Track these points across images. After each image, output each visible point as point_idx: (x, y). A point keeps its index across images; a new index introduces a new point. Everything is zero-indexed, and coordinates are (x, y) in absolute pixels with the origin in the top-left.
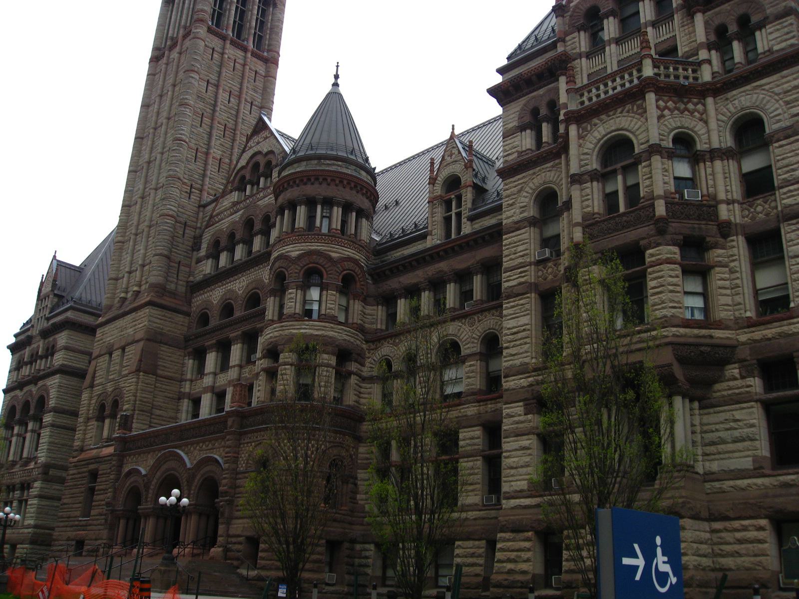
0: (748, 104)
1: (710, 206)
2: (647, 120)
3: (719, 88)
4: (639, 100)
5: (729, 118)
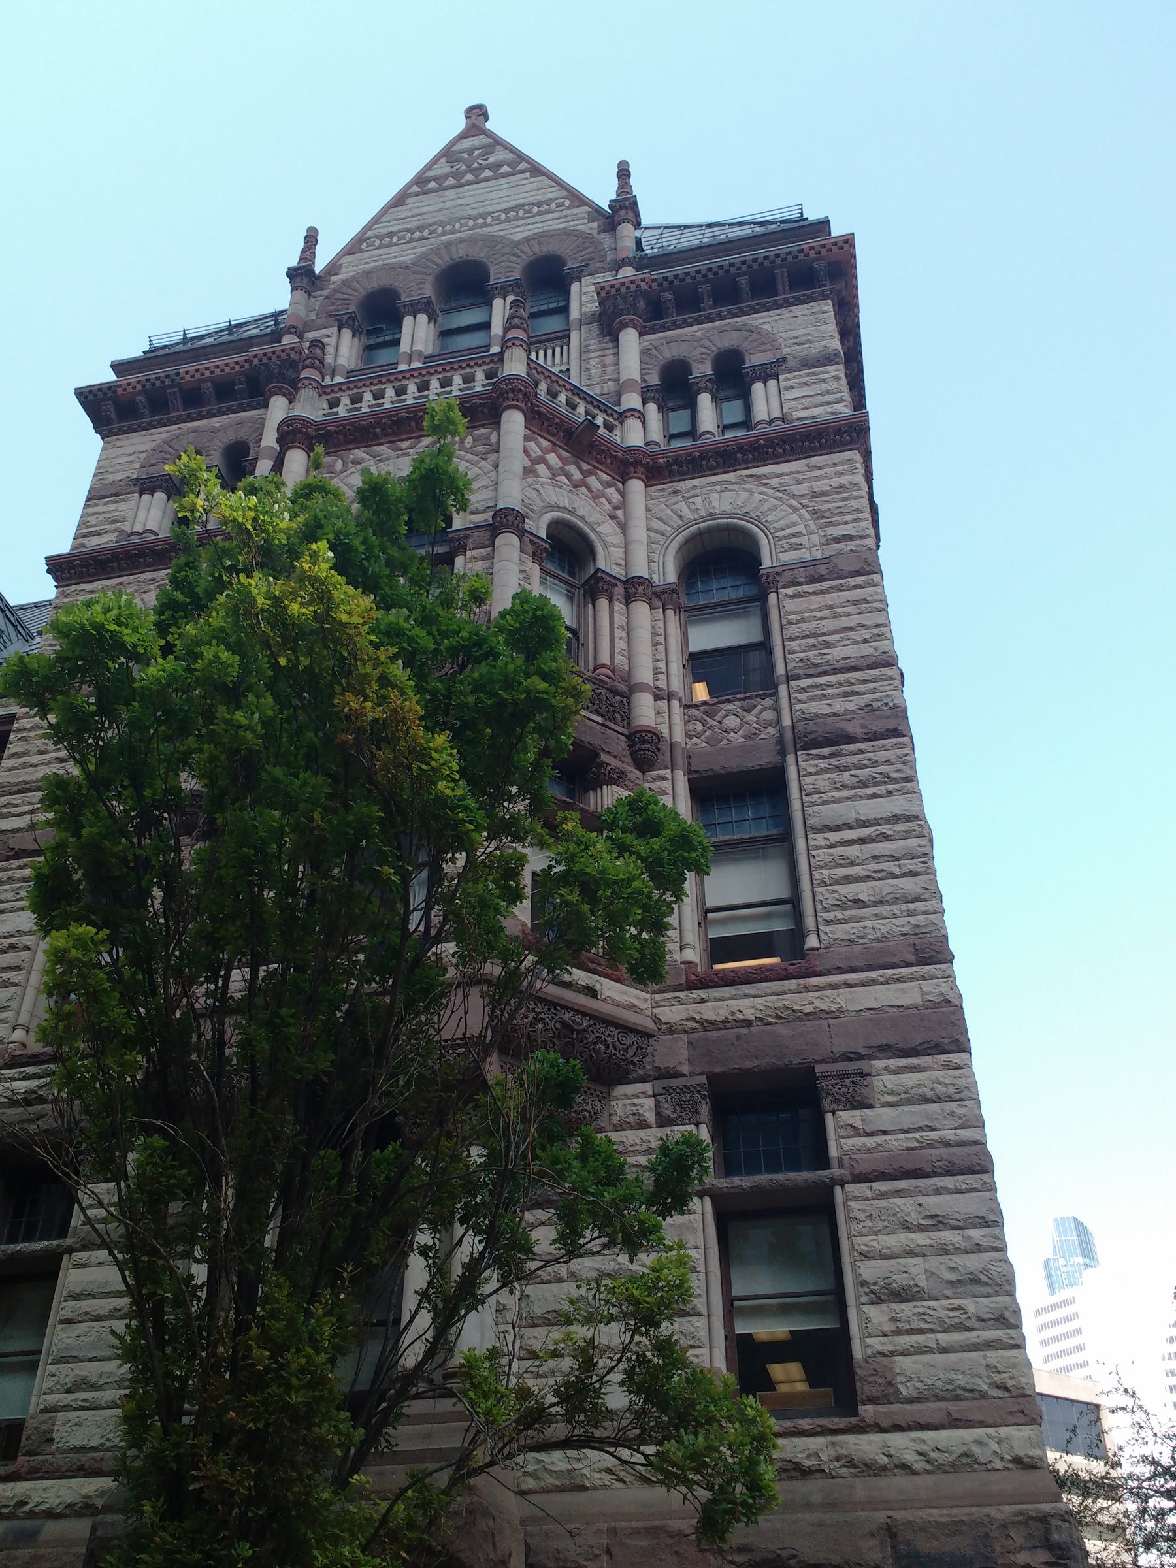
0: (727, 508)
1: (616, 693)
2: (496, 467)
3: (658, 469)
4: (482, 426)
5: (678, 530)
